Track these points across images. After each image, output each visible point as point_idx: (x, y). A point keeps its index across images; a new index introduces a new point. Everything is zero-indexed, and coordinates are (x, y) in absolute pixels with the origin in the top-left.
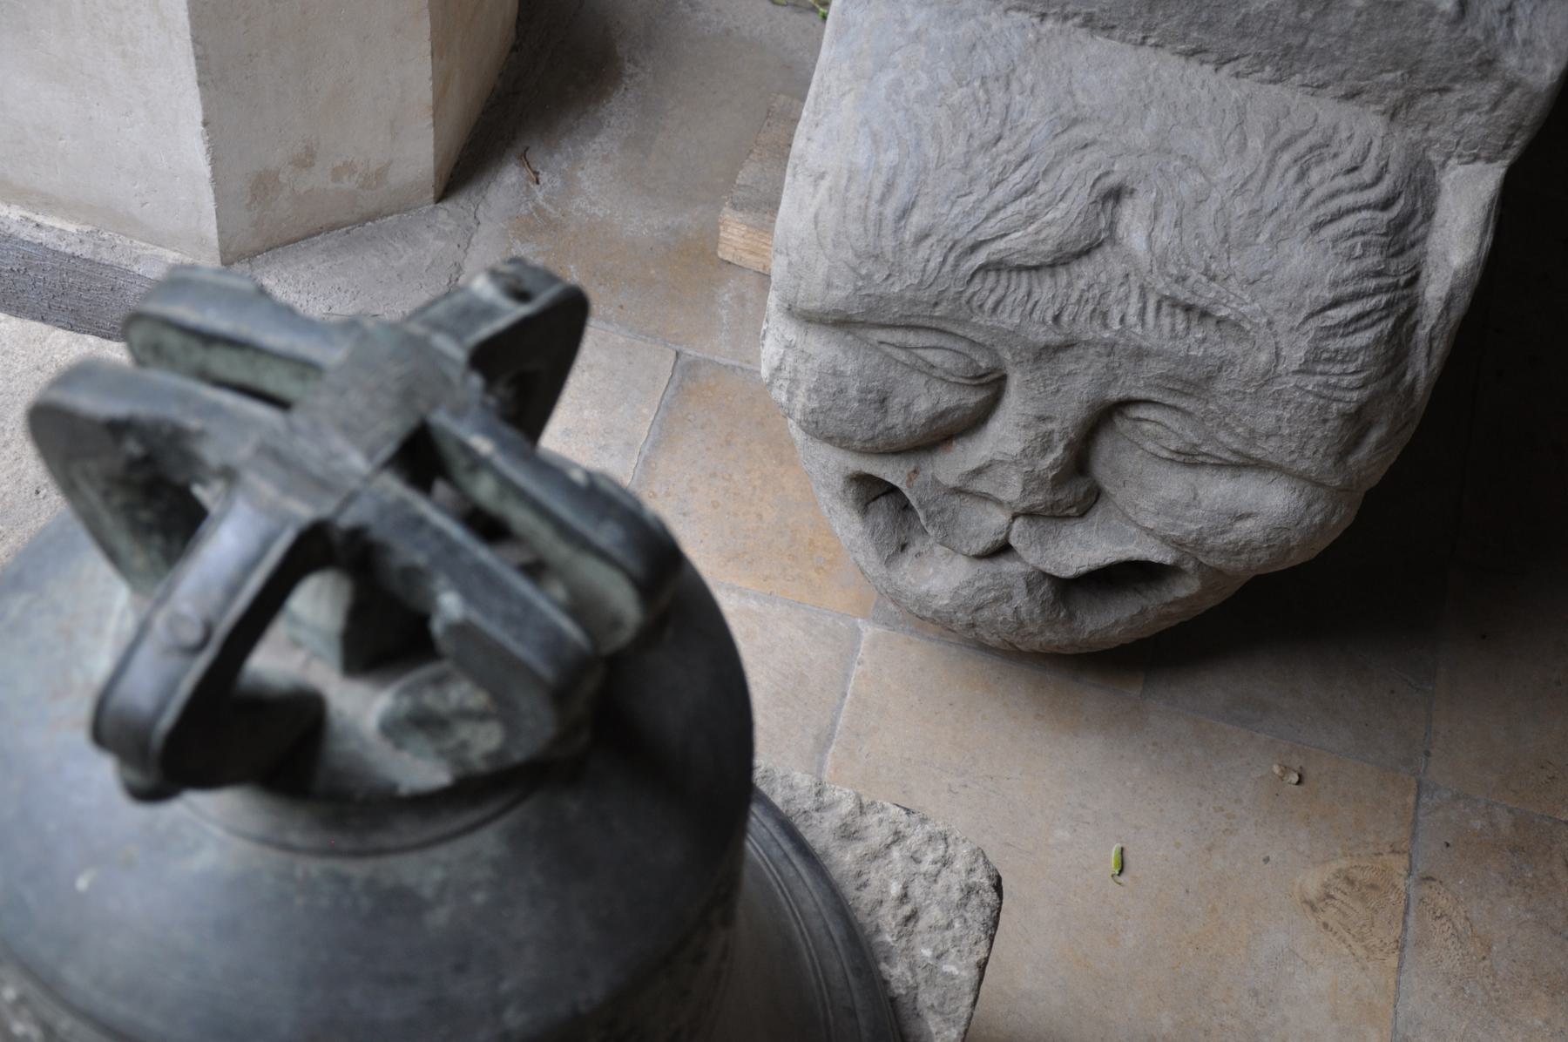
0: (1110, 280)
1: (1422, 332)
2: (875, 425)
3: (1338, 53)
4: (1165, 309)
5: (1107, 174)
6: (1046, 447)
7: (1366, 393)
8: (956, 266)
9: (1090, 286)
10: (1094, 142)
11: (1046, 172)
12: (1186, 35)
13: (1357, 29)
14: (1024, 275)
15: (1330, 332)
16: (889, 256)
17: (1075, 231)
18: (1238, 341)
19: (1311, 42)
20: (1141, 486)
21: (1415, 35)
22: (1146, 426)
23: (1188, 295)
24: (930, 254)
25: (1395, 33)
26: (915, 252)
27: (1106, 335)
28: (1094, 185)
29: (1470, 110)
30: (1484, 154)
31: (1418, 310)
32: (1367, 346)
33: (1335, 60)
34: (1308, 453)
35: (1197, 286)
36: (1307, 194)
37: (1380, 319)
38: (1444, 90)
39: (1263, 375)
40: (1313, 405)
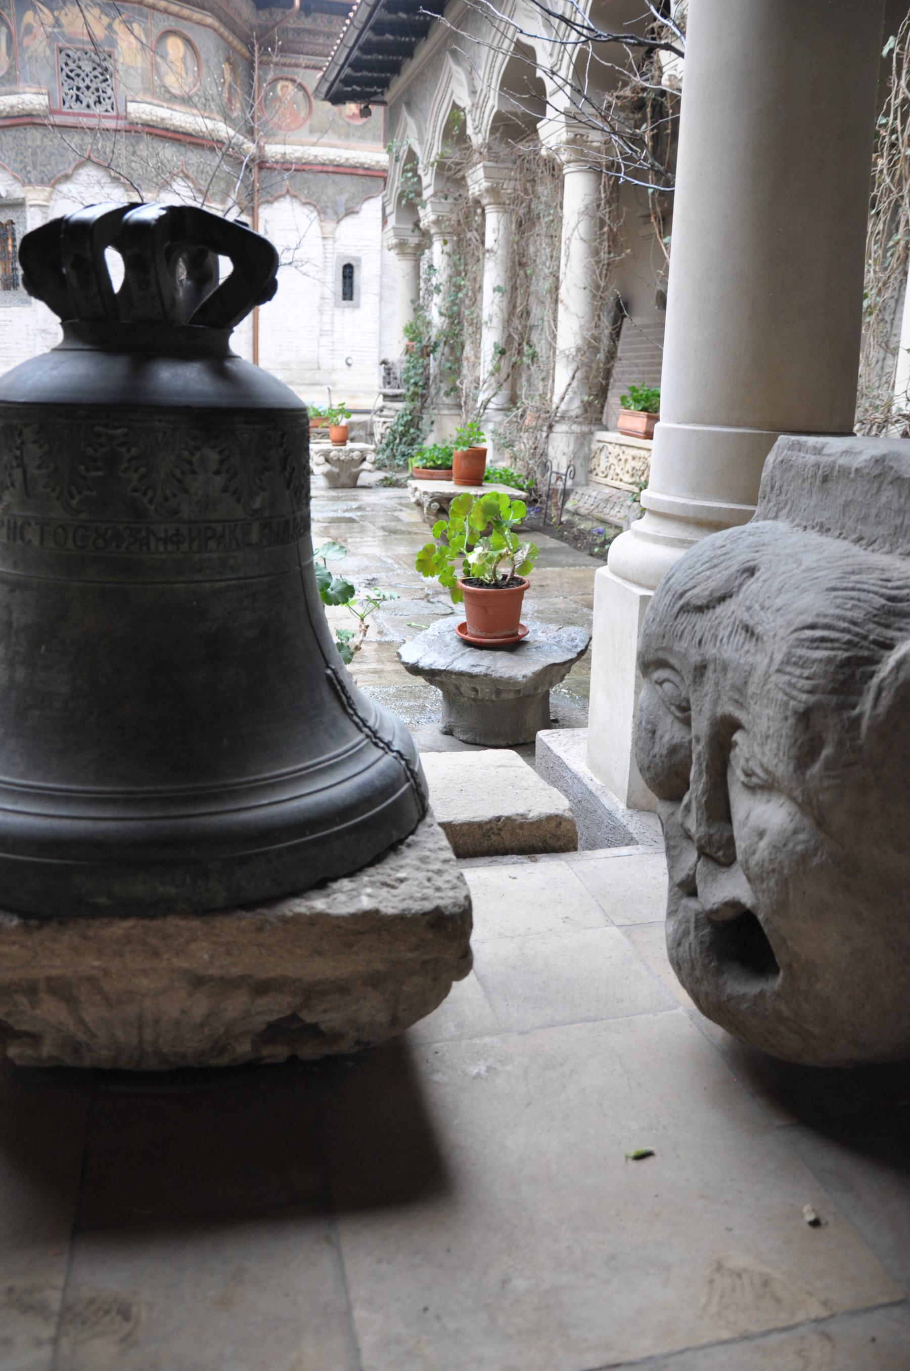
0: (726, 615)
4: (739, 630)
7: (812, 699)
12: (856, 528)
17: (721, 583)
32: (821, 661)
34: (781, 754)
37: (839, 649)
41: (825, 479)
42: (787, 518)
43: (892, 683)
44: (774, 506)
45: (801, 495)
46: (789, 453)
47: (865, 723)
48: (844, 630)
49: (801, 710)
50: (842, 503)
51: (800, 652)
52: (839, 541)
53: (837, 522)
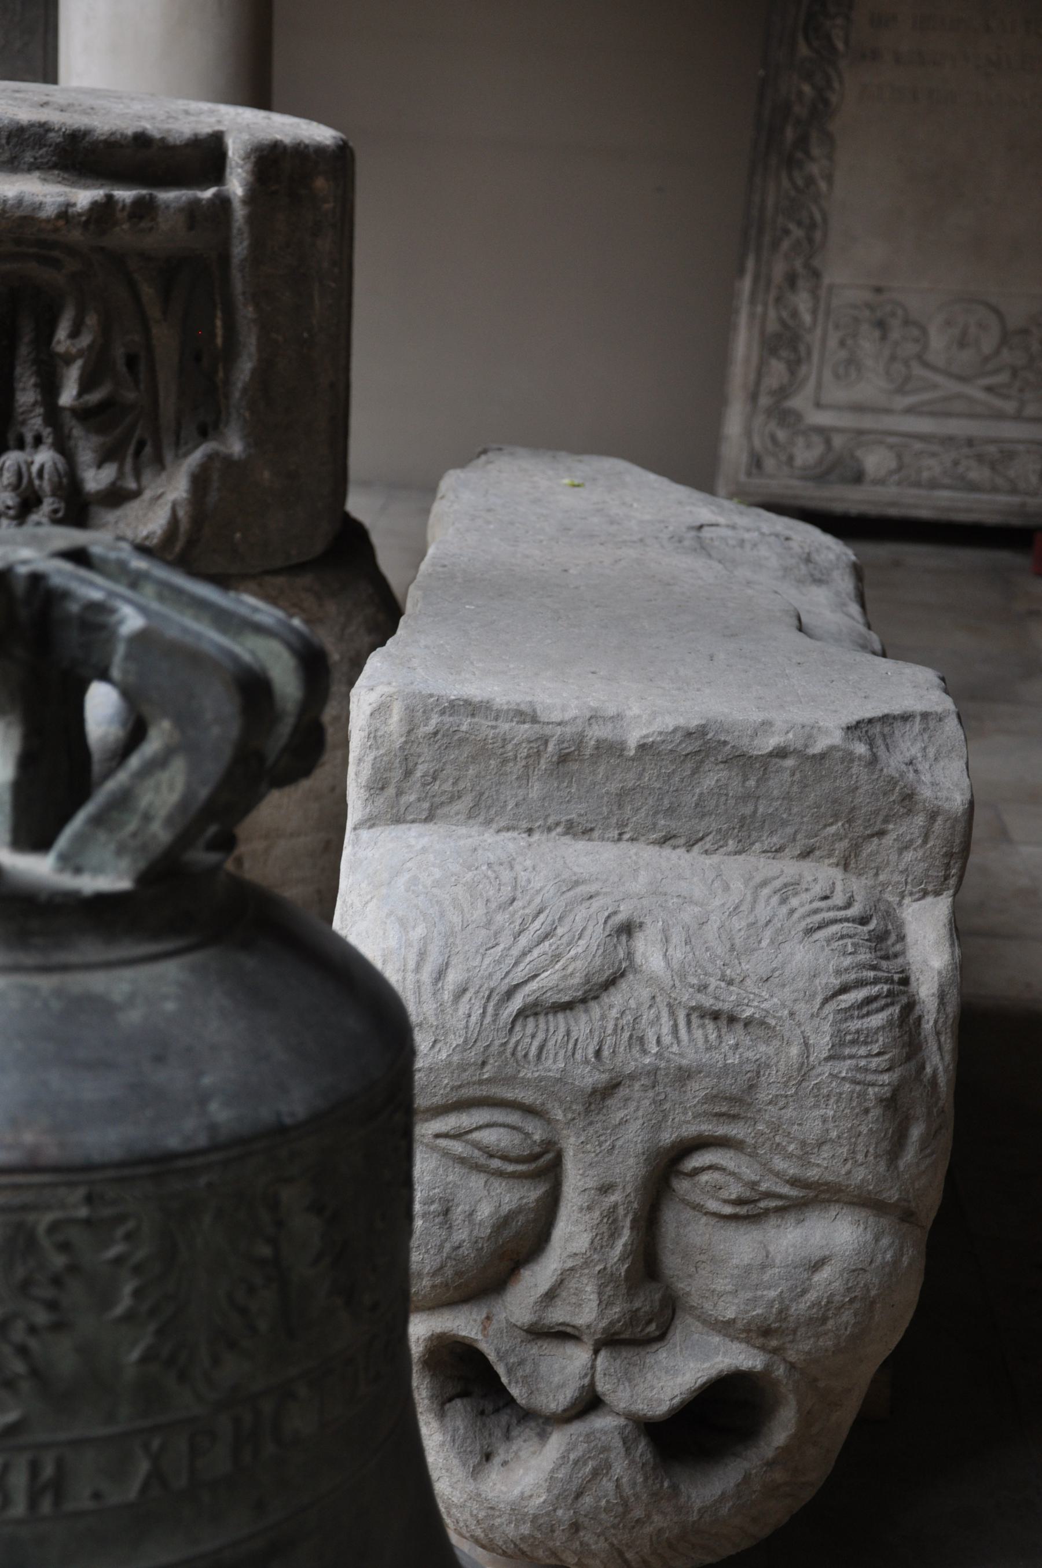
0: (639, 1005)
1: (928, 1026)
2: (441, 1247)
3: (785, 816)
4: (694, 1018)
5: (615, 913)
6: (614, 1234)
8: (496, 1015)
9: (623, 1013)
10: (597, 894)
11: (561, 919)
12: (655, 824)
13: (795, 789)
14: (561, 1017)
15: (847, 1013)
16: (432, 1020)
17: (598, 961)
18: (767, 1042)
19: (761, 810)
20: (713, 1260)
21: (843, 783)
22: (704, 1177)
23: (712, 1001)
24: (471, 1006)
25: (827, 785)
26: (456, 1010)
27: (647, 1061)
28: (605, 922)
29: (906, 848)
30: (930, 888)
31: (918, 1007)
32: (883, 1027)
33: (784, 823)
34: (860, 1157)
35: (718, 991)
36: (792, 911)
38: (881, 833)
39: (800, 1069)
40: (853, 1092)
41: (563, 759)
42: (469, 818)
43: (945, 1023)
44: (419, 800)
45: (500, 784)
46: (447, 719)
47: (942, 1080)
48: (876, 981)
49: (888, 1095)
50: (613, 790)
51: (855, 1025)
52: (623, 845)
53: (607, 818)
